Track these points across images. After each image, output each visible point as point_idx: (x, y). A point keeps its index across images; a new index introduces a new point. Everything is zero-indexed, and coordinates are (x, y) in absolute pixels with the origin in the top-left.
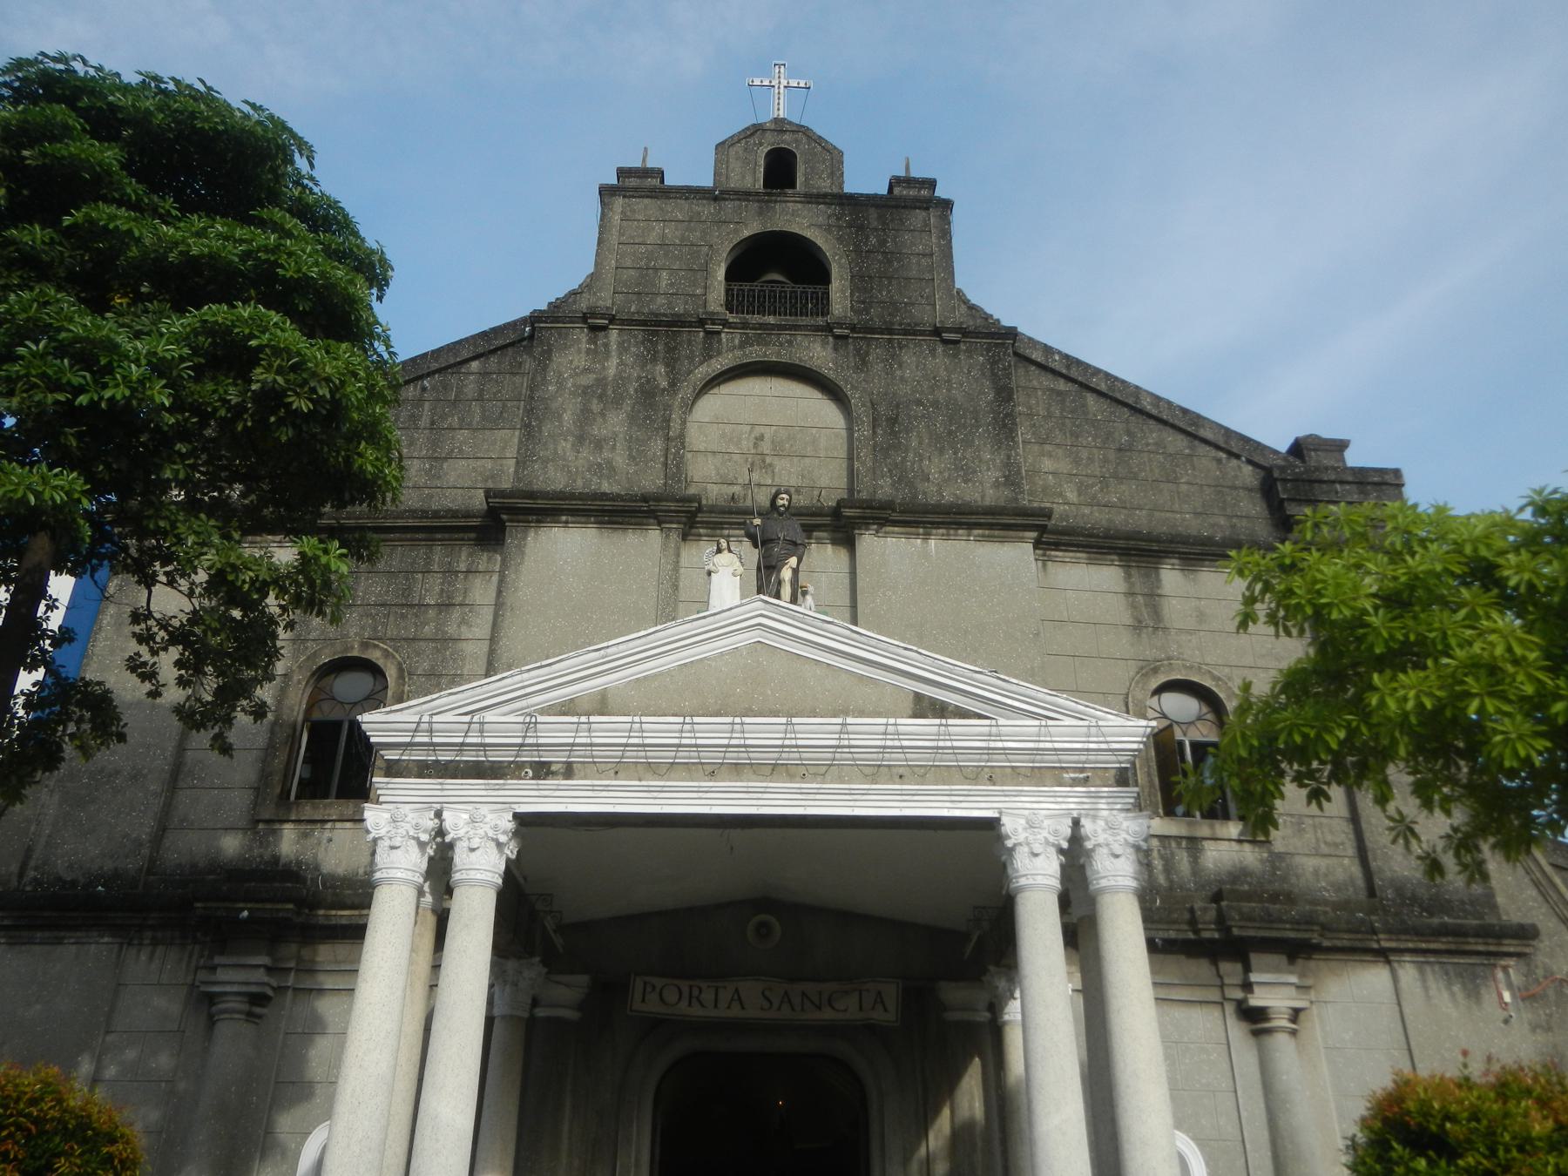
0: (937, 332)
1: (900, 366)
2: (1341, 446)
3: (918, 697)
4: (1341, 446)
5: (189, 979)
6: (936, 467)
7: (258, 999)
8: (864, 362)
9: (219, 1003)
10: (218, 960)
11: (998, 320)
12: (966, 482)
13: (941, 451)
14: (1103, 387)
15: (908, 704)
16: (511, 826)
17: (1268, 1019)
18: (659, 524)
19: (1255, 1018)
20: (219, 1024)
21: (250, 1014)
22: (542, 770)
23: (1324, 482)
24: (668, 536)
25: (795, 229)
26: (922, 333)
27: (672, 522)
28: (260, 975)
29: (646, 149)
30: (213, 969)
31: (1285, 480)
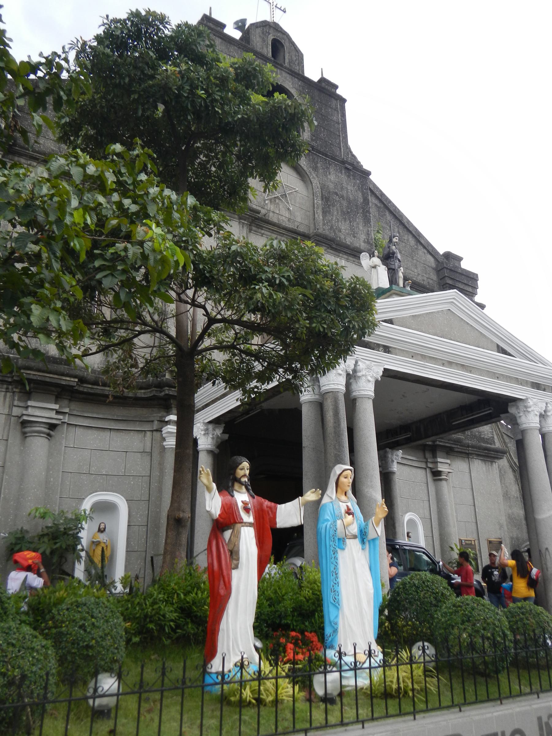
0: (343, 162)
1: (330, 174)
2: (459, 259)
3: (498, 346)
4: (459, 259)
5: (6, 411)
6: (344, 226)
7: (52, 427)
8: (317, 167)
9: (31, 427)
10: (30, 403)
11: (362, 166)
12: (354, 237)
13: (345, 219)
14: (391, 209)
15: (496, 348)
16: (381, 374)
17: (440, 475)
18: (240, 218)
19: (436, 474)
20: (28, 439)
21: (49, 435)
22: (387, 349)
23: (457, 272)
24: (243, 227)
25: (288, 88)
26: (338, 161)
27: (245, 220)
28: (53, 415)
29: (211, 8)
30: (27, 407)
31: (447, 268)
